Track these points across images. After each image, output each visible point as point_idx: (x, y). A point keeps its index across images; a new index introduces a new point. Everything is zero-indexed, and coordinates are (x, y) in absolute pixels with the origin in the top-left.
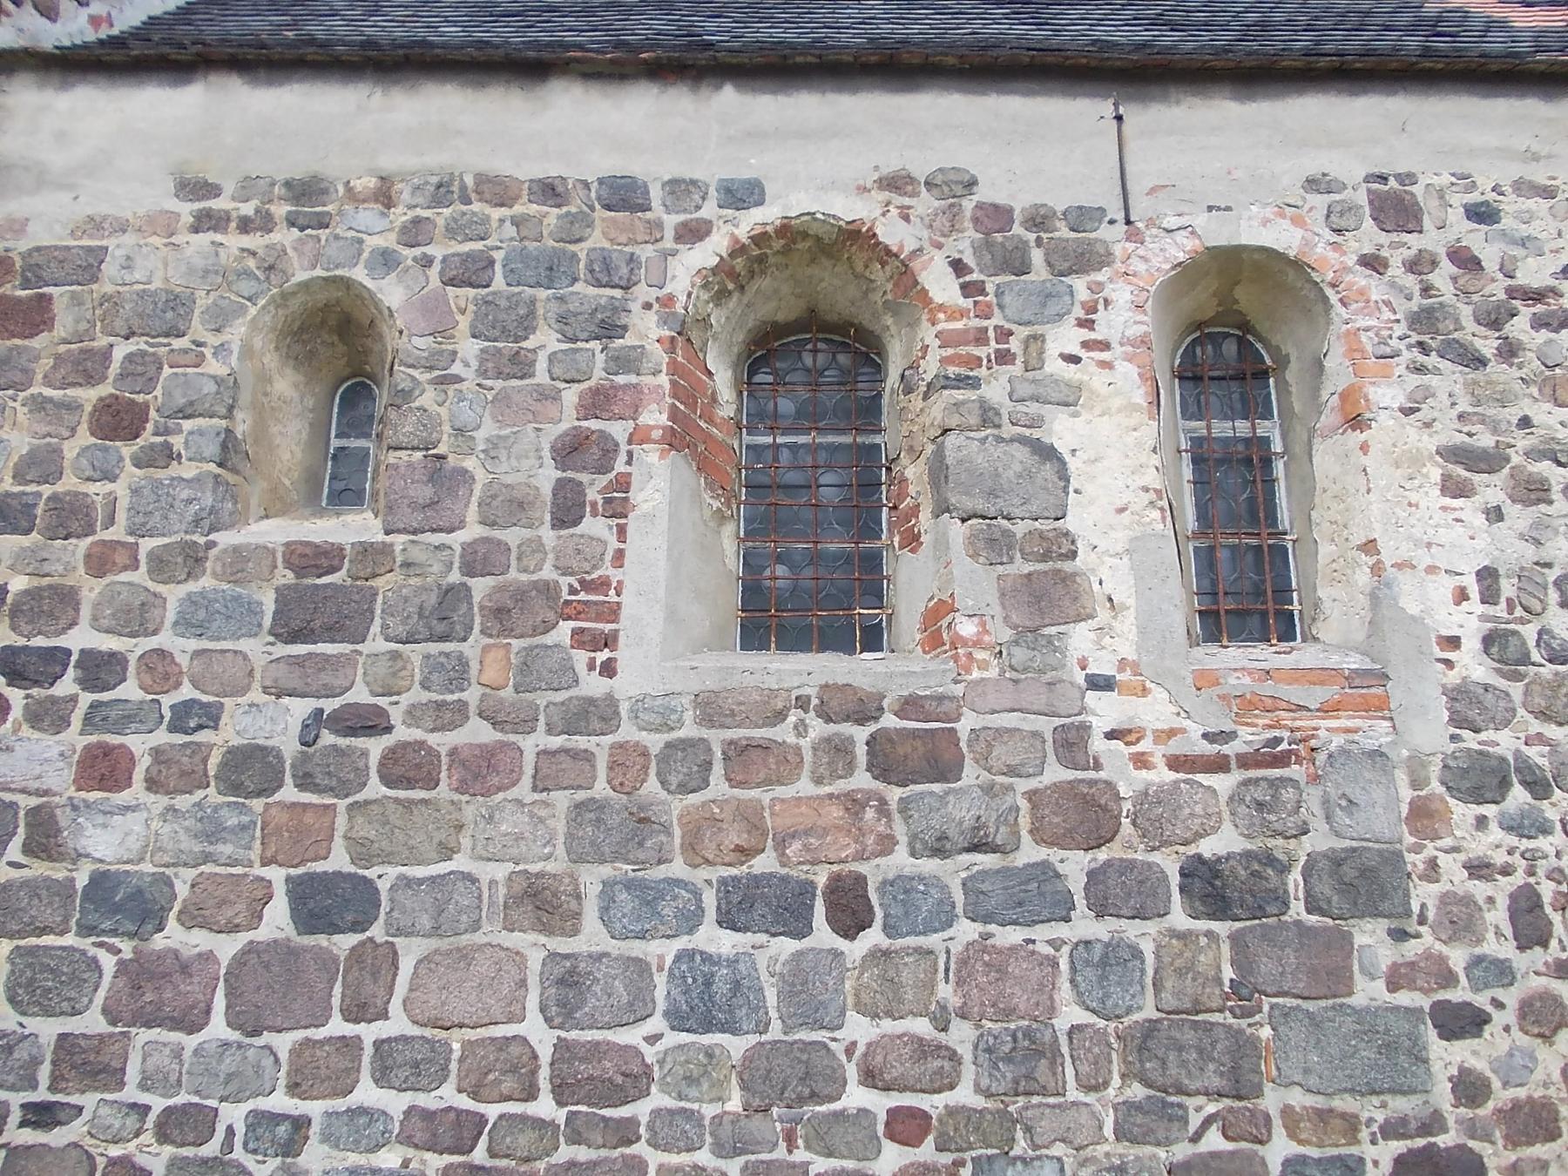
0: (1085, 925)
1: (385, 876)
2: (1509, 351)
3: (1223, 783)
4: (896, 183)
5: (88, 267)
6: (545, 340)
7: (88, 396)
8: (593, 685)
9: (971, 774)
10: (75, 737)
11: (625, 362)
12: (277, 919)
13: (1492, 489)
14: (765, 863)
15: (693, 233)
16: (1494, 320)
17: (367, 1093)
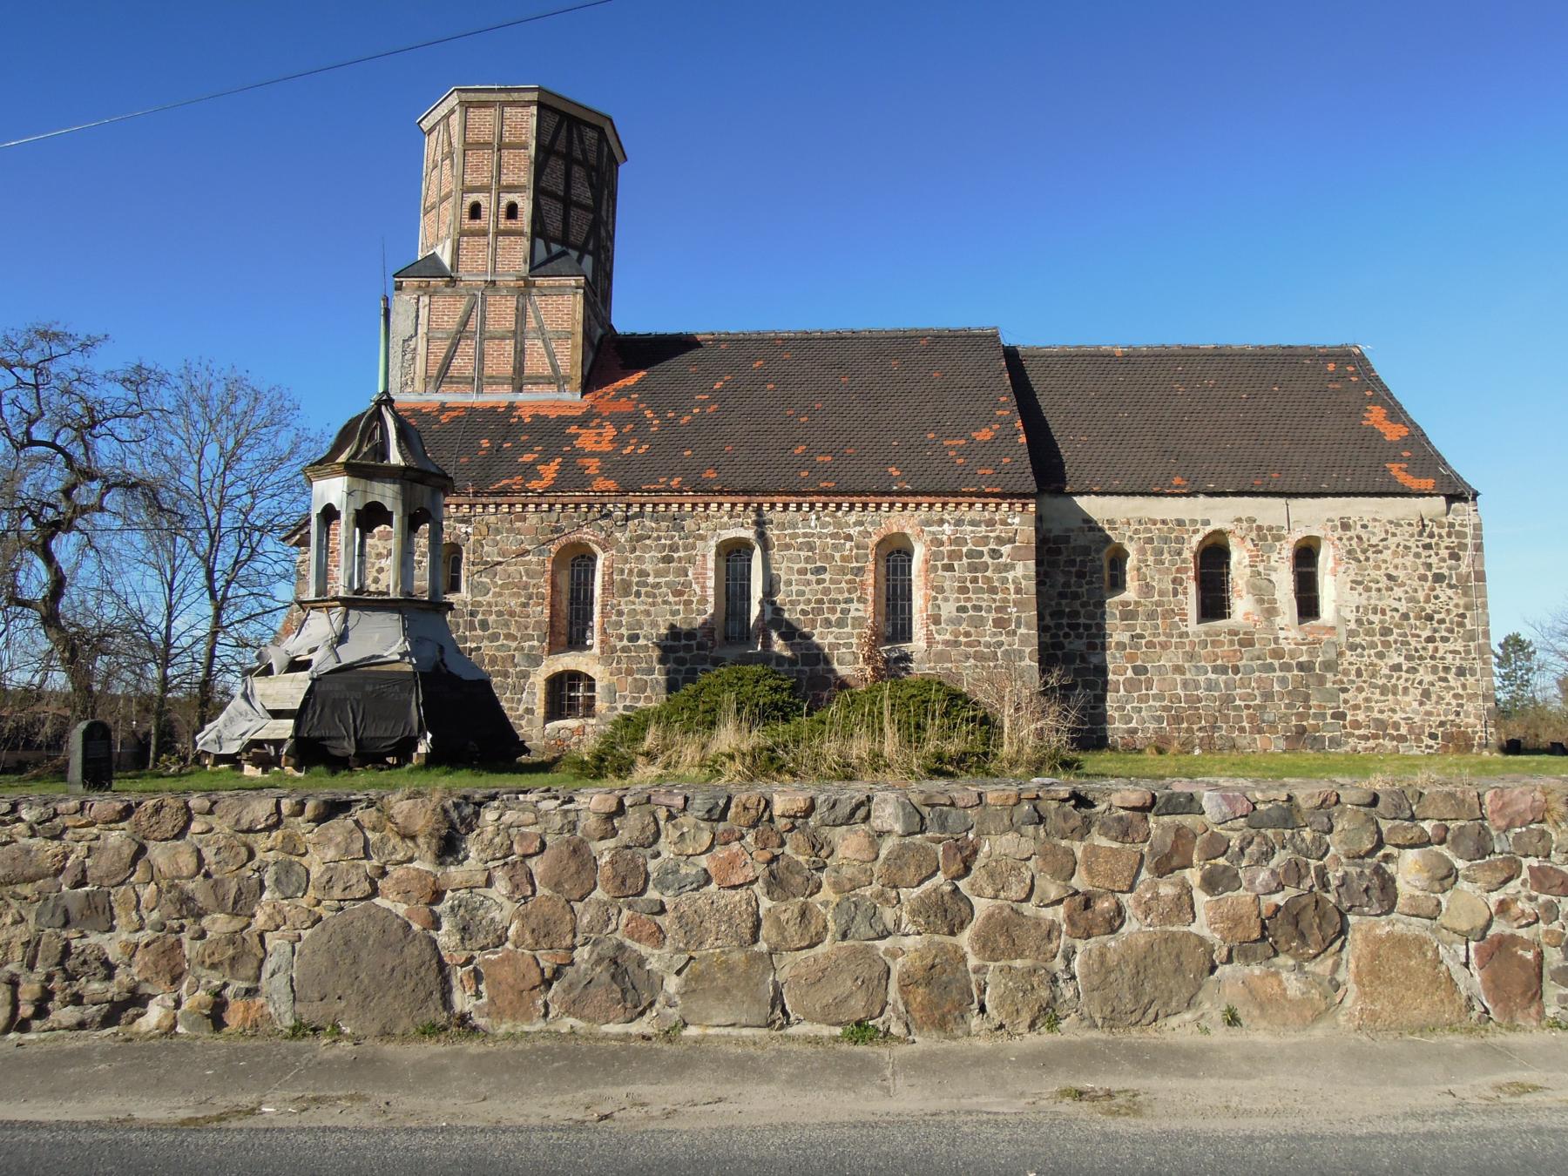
0: (1278, 673)
1: (1149, 666)
2: (1367, 559)
3: (1304, 648)
4: (1239, 520)
5: (1067, 539)
6: (1166, 556)
7: (1074, 570)
8: (1184, 629)
9: (1257, 646)
10: (1085, 640)
11: (1184, 561)
12: (1130, 673)
13: (1360, 588)
14: (1219, 662)
15: (1196, 532)
16: (1364, 551)
17: (1151, 703)
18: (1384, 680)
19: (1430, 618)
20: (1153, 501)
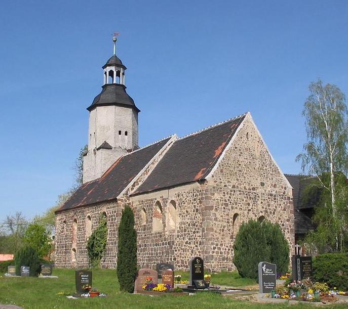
18: (184, 247)
19: (194, 225)
20: (145, 195)
